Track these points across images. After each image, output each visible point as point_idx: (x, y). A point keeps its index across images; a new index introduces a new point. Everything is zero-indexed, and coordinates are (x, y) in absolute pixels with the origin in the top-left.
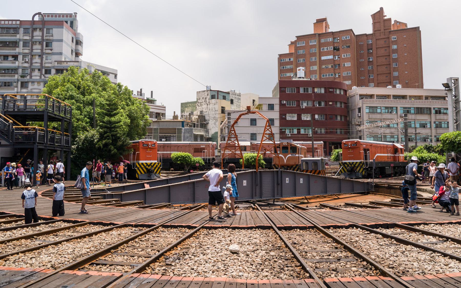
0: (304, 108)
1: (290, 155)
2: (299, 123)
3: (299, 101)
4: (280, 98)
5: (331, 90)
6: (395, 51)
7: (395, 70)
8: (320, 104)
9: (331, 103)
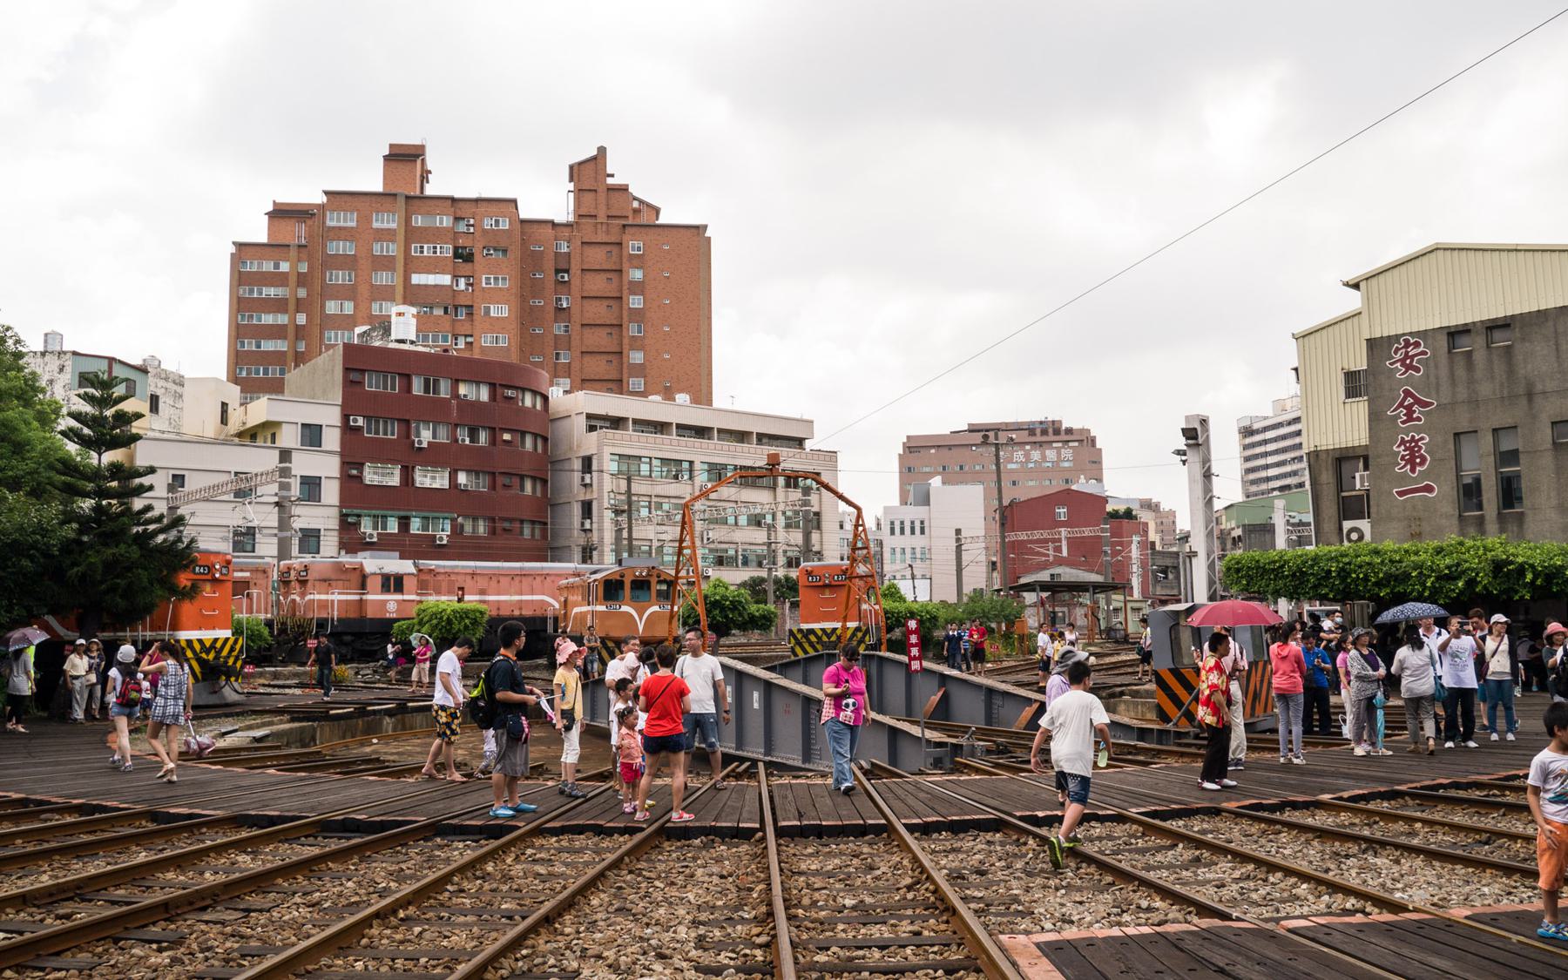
0: (425, 445)
1: (656, 608)
2: (406, 498)
3: (408, 422)
4: (344, 406)
5: (510, 393)
6: (637, 288)
7: (637, 344)
8: (473, 435)
9: (507, 437)
